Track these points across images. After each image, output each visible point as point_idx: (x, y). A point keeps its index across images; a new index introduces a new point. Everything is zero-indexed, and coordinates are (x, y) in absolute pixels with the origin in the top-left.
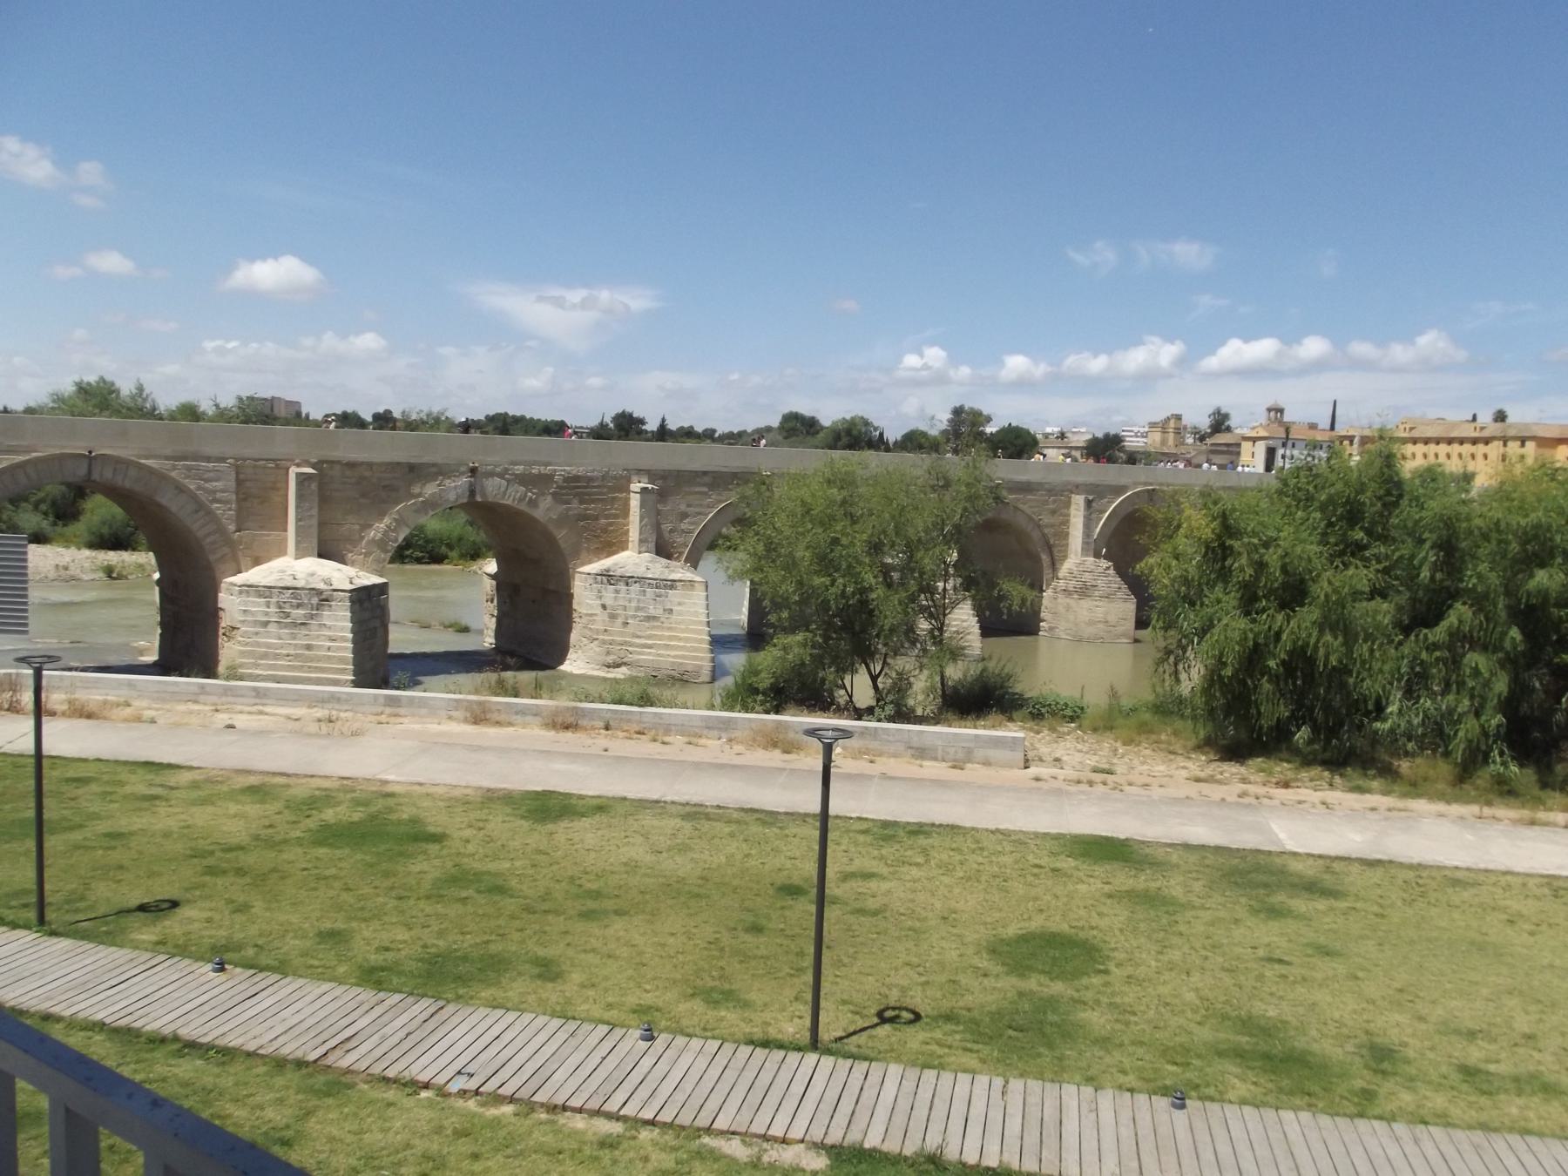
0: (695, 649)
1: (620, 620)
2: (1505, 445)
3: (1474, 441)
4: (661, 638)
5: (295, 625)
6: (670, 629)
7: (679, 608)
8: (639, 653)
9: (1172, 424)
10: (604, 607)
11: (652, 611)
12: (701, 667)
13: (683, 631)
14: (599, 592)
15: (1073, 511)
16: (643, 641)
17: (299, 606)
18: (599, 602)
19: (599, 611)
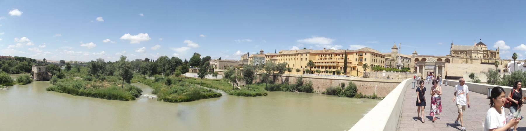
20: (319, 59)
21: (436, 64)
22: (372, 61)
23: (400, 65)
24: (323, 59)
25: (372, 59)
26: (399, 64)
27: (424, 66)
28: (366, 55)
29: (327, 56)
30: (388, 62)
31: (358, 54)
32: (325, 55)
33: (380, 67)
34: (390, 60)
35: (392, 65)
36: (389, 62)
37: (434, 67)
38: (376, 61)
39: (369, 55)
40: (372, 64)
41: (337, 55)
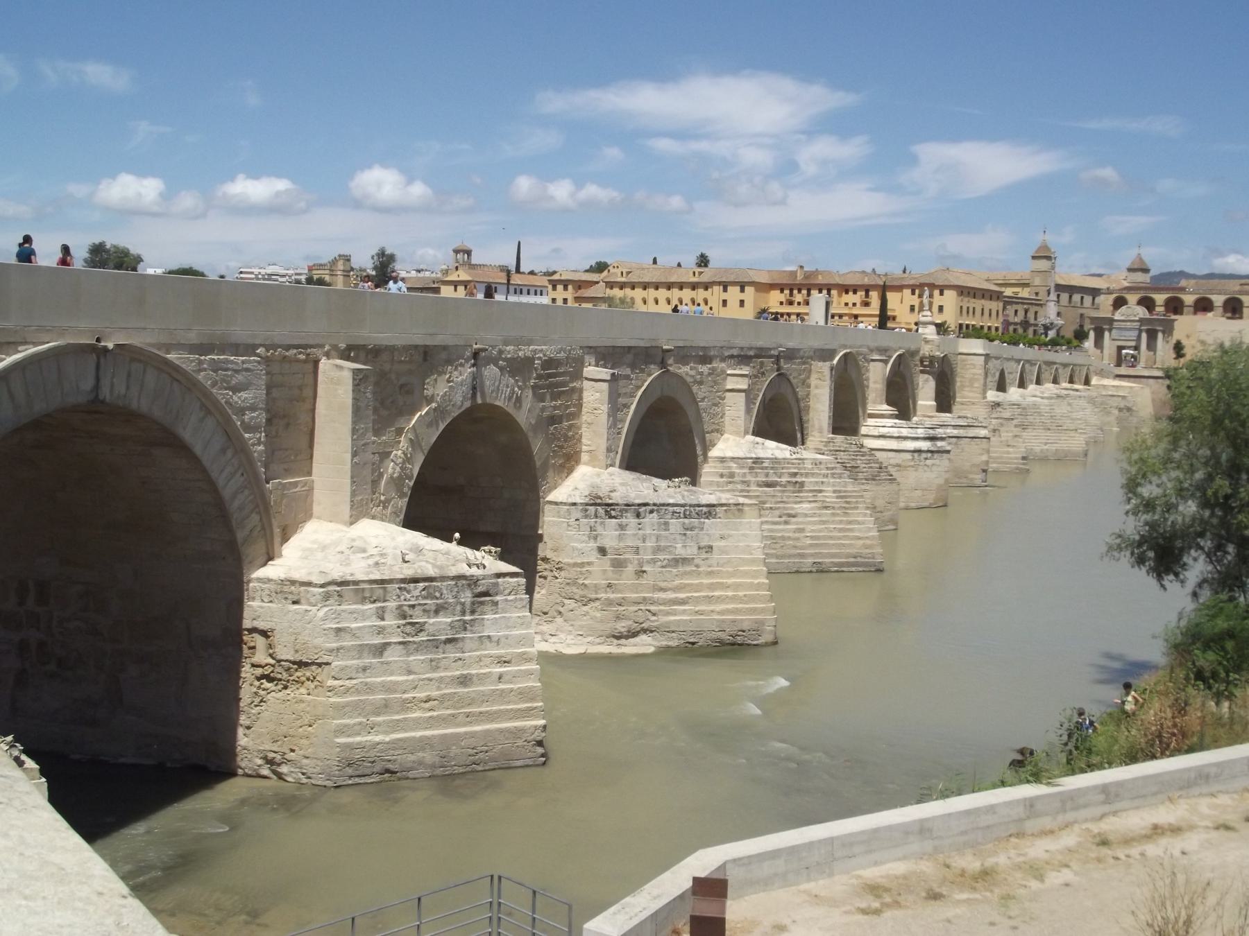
0: (752, 599)
1: (630, 569)
2: (725, 290)
3: (694, 286)
4: (698, 588)
5: (435, 644)
6: (710, 574)
7: (722, 543)
8: (668, 613)
9: (340, 266)
10: (602, 551)
11: (680, 551)
12: (762, 622)
13: (732, 575)
15: (813, 381)
16: (671, 595)
17: (437, 611)
18: (593, 545)
19: (594, 557)
20: (781, 303)
21: (1141, 326)
22: (961, 312)
23: (1052, 324)
25: (961, 307)
26: (1048, 321)
27: (1110, 330)
28: (942, 294)
30: (1016, 311)
31: (917, 292)
32: (804, 292)
33: (986, 330)
34: (1023, 301)
35: (1032, 321)
36: (1021, 309)
37: (1136, 333)
38: (974, 313)
39: (950, 295)
40: (960, 322)
41: (847, 292)
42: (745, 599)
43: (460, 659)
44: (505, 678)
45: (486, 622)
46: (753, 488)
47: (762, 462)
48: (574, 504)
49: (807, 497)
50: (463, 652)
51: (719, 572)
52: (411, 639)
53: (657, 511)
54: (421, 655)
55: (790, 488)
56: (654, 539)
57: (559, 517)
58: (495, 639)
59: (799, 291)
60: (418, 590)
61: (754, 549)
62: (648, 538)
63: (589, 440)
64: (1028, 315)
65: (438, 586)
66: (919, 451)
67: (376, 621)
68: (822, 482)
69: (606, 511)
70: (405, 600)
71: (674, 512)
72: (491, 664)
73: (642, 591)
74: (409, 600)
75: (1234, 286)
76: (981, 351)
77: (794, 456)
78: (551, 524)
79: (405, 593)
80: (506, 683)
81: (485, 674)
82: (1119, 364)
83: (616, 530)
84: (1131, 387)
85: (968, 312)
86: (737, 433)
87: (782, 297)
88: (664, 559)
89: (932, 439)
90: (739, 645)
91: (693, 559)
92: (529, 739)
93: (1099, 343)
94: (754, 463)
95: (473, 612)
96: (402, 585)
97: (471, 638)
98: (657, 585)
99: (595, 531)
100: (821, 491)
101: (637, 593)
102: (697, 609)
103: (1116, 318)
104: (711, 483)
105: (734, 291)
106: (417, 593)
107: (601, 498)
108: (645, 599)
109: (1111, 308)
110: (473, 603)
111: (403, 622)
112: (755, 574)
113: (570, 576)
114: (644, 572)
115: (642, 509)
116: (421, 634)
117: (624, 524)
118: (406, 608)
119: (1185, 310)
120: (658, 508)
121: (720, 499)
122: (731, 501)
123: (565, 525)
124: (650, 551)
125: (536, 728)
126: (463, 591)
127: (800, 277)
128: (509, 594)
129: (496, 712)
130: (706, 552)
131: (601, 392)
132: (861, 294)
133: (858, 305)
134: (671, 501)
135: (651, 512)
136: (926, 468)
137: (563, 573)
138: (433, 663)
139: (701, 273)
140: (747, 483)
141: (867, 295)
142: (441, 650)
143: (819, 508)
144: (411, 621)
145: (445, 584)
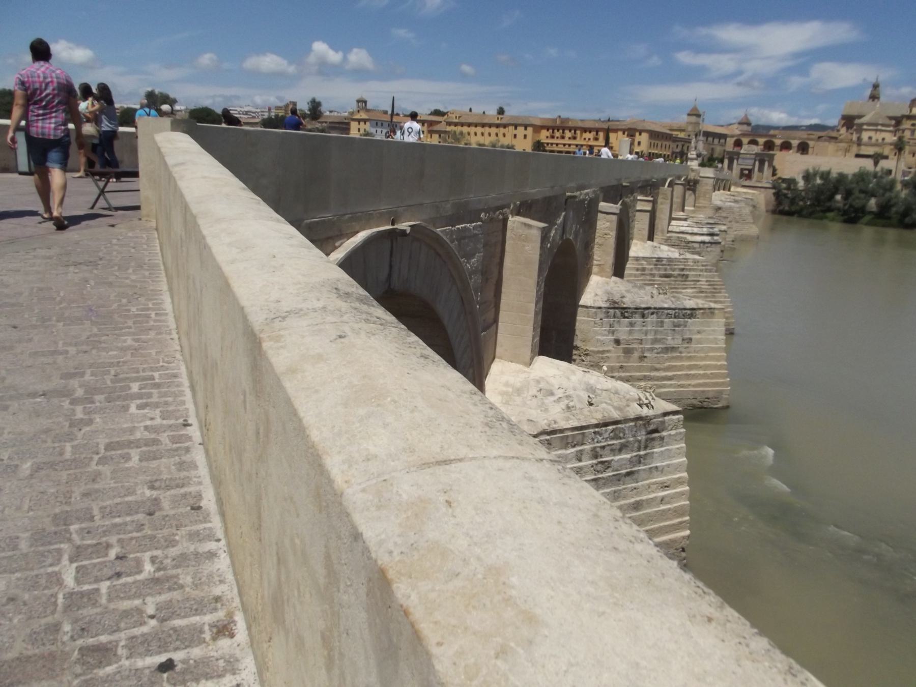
1: (636, 355)
2: (516, 128)
3: (498, 126)
4: (681, 368)
5: (618, 479)
6: (690, 358)
7: (699, 336)
10: (617, 342)
11: (670, 342)
12: (721, 392)
13: (703, 359)
14: (611, 326)
16: (663, 374)
17: (622, 448)
18: (611, 337)
20: (547, 137)
24: (557, 138)
27: (738, 159)
28: (640, 134)
29: (567, 132)
30: (677, 146)
32: (561, 131)
34: (681, 140)
36: (680, 144)
37: (753, 161)
40: (650, 151)
41: (585, 132)
42: (711, 376)
43: (635, 488)
44: (666, 500)
45: (655, 455)
46: (657, 278)
47: (662, 261)
48: (600, 308)
49: (691, 285)
50: (637, 482)
51: (695, 357)
52: (600, 476)
53: (657, 313)
54: (607, 488)
55: (680, 279)
56: (653, 333)
57: (589, 317)
58: (660, 469)
59: (558, 130)
60: (608, 433)
61: (719, 341)
62: (649, 333)
63: (599, 257)
64: (684, 148)
65: (623, 428)
66: (703, 242)
67: (575, 463)
68: (700, 275)
69: (622, 313)
70: (597, 442)
71: (668, 314)
72: (656, 489)
73: (642, 372)
74: (601, 442)
75: (803, 135)
76: (712, 175)
77: (682, 257)
78: (582, 320)
79: (598, 436)
80: (669, 503)
81: (652, 499)
82: (741, 178)
83: (627, 327)
84: (754, 194)
85: (665, 147)
86: (642, 240)
87: (548, 134)
88: (659, 348)
89: (712, 235)
90: (705, 408)
91: (679, 347)
92: (678, 547)
93: (730, 167)
94: (657, 261)
95: (646, 448)
96: (597, 430)
97: (644, 470)
98: (653, 366)
99: (613, 327)
100: (698, 281)
101: (640, 372)
102: (679, 383)
103: (742, 151)
104: (631, 275)
105: (521, 130)
106: (606, 435)
107: (616, 303)
108: (645, 376)
109: (732, 146)
110: (647, 440)
111: (595, 461)
112: (718, 359)
113: (594, 360)
114: (645, 357)
115: (646, 312)
116: (607, 471)
117: (633, 322)
118: (598, 449)
119: (775, 148)
120: (657, 311)
121: (697, 304)
122: (706, 306)
123: (593, 323)
124: (650, 342)
125: (684, 538)
126: (640, 430)
127: (558, 122)
128: (671, 429)
129: (657, 529)
130: (688, 343)
131: (611, 222)
132: (594, 133)
133: (592, 139)
134: (666, 306)
135: (652, 314)
136: (707, 253)
137: (588, 358)
138: (616, 494)
139: (501, 118)
140: (653, 275)
141: (597, 134)
142: (621, 482)
143: (697, 292)
144: (602, 460)
145: (627, 425)
